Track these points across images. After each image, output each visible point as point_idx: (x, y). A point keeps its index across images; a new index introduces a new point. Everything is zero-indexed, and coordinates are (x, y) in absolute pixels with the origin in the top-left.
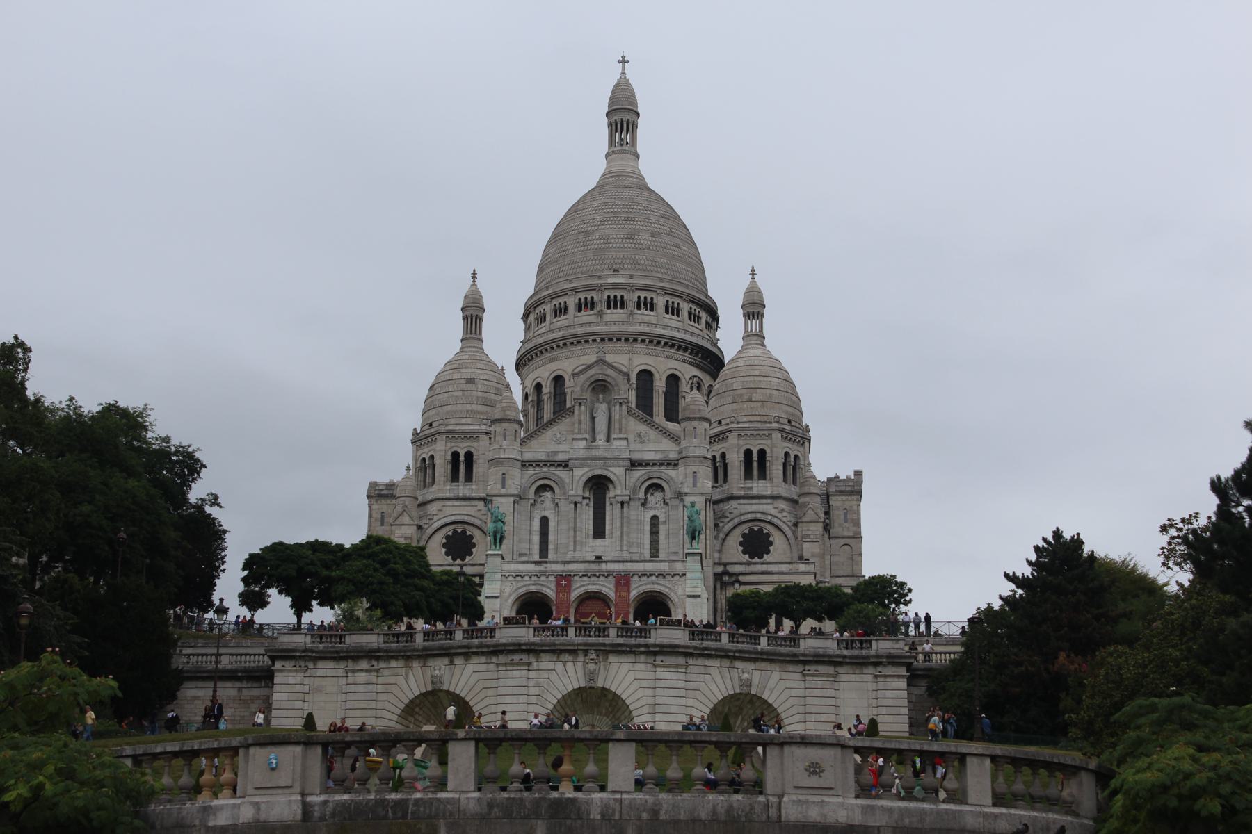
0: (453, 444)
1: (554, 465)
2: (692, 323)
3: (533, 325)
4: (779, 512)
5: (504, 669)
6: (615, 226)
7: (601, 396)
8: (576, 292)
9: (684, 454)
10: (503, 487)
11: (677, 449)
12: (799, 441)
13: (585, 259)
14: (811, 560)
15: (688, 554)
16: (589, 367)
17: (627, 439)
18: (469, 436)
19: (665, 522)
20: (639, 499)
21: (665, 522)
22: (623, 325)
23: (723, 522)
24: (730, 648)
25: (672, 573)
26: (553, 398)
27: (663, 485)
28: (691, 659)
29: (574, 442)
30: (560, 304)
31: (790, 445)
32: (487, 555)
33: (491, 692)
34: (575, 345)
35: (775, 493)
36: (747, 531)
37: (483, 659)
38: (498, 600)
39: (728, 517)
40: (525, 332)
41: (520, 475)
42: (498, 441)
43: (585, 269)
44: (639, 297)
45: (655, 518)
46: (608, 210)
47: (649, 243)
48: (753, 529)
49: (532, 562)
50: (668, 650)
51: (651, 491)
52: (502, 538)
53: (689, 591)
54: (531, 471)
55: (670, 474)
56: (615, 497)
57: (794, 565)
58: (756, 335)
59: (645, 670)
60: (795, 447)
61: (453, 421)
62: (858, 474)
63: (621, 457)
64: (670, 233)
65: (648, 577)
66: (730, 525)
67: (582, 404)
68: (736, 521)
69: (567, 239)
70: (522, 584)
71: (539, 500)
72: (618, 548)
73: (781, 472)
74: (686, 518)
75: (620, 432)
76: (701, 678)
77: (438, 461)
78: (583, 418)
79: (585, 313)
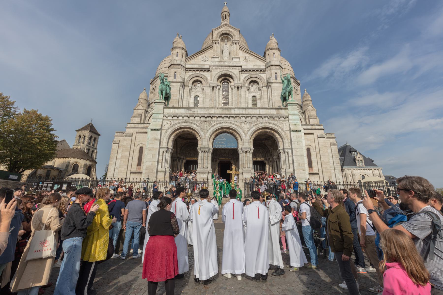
1: (202, 70)
7: (226, 41)
9: (269, 64)
10: (175, 78)
17: (239, 58)
19: (260, 99)
20: (246, 87)
25: (279, 116)
29: (212, 59)
42: (174, 57)
51: (251, 84)
53: (293, 128)
54: (190, 73)
55: (262, 76)
56: (234, 85)
60: (296, 87)
67: (217, 43)
70: (177, 122)
71: (194, 88)
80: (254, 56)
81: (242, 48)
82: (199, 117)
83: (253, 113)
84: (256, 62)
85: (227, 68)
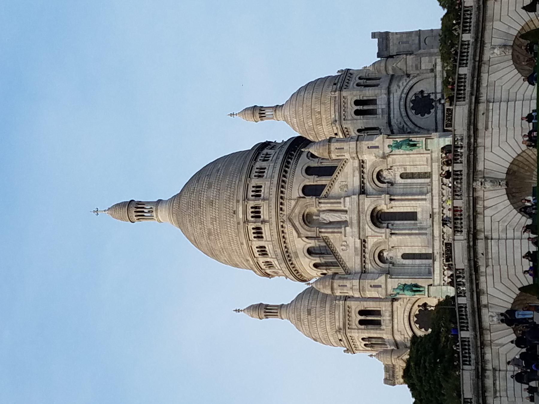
0: (354, 324)
1: (364, 250)
2: (270, 159)
3: (273, 270)
4: (399, 88)
5: (490, 260)
6: (204, 214)
8: (249, 240)
10: (380, 286)
11: (351, 161)
12: (349, 76)
13: (227, 234)
14: (434, 63)
15: (426, 148)
16: (294, 226)
18: (348, 313)
19: (405, 169)
20: (388, 187)
21: (405, 169)
22: (271, 206)
24: (472, 64)
26: (323, 255)
27: (378, 171)
28: (481, 98)
29: (347, 235)
30: (258, 251)
31: (352, 83)
32: (429, 297)
33: (512, 272)
34: (286, 239)
36: (414, 111)
37: (482, 279)
39: (403, 126)
40: (280, 275)
41: (372, 274)
43: (234, 234)
44: (252, 196)
45: (402, 176)
46: (194, 219)
47: (215, 190)
49: (434, 264)
50: (473, 117)
51: (382, 179)
52: (416, 286)
54: (369, 266)
55: (370, 164)
56: (387, 205)
57: (437, 74)
58: (275, 111)
59: (490, 138)
60: (353, 79)
61: (337, 324)
62: (374, 35)
64: (209, 176)
66: (409, 123)
67: (320, 230)
68: (406, 119)
69: (214, 247)
72: (424, 202)
73: (371, 88)
74: (401, 151)
75: (340, 203)
76: (498, 89)
77: (366, 335)
78: (330, 230)
79: (264, 233)
80: (338, 175)
81: (325, 193)
83: (437, 188)
84: (347, 172)
85: (361, 215)
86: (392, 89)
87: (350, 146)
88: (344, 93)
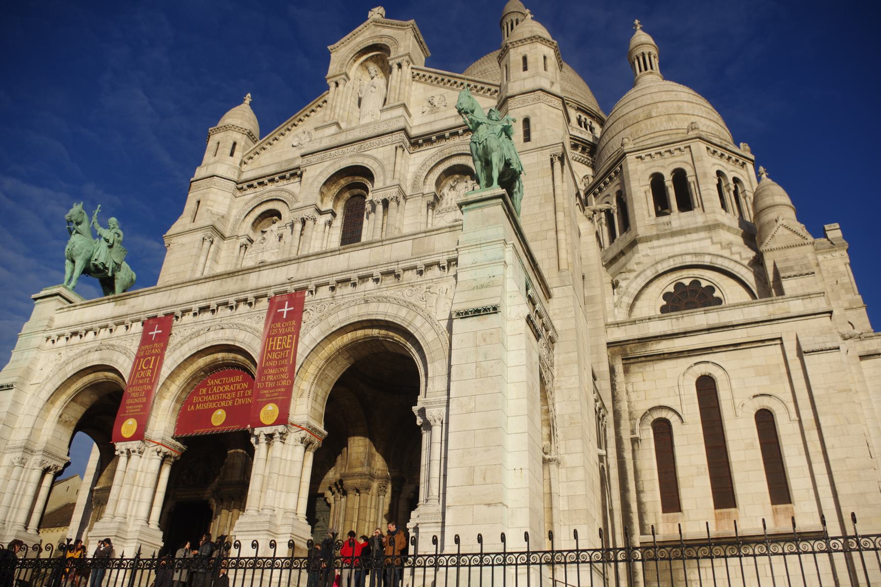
1: (283, 178)
2: (584, 129)
12: (737, 161)
23: (626, 279)
25: (420, 264)
35: (710, 223)
36: (671, 289)
38: (12, 392)
39: (634, 271)
41: (228, 201)
48: (681, 283)
54: (250, 194)
58: (651, 73)
60: (732, 168)
63: (390, 130)
65: (354, 285)
66: (641, 282)
67: (341, 83)
68: (650, 274)
70: (76, 351)
82: (140, 324)
83: (326, 270)
86: (721, 231)
87: (526, 80)
88: (700, 147)
